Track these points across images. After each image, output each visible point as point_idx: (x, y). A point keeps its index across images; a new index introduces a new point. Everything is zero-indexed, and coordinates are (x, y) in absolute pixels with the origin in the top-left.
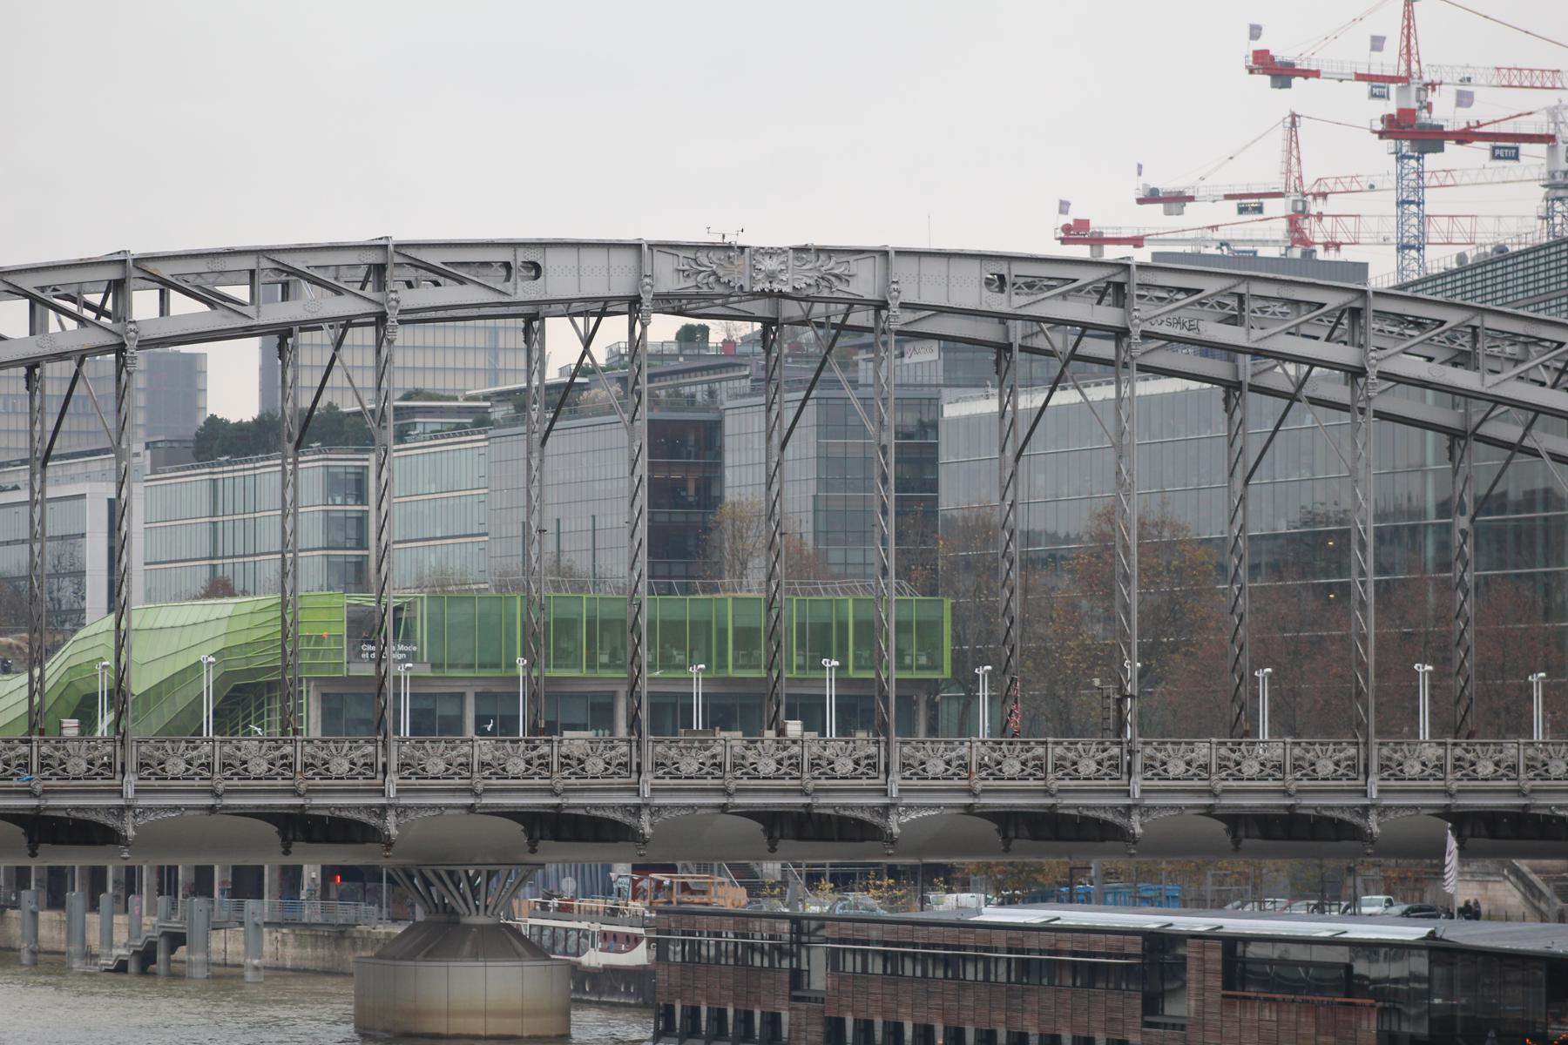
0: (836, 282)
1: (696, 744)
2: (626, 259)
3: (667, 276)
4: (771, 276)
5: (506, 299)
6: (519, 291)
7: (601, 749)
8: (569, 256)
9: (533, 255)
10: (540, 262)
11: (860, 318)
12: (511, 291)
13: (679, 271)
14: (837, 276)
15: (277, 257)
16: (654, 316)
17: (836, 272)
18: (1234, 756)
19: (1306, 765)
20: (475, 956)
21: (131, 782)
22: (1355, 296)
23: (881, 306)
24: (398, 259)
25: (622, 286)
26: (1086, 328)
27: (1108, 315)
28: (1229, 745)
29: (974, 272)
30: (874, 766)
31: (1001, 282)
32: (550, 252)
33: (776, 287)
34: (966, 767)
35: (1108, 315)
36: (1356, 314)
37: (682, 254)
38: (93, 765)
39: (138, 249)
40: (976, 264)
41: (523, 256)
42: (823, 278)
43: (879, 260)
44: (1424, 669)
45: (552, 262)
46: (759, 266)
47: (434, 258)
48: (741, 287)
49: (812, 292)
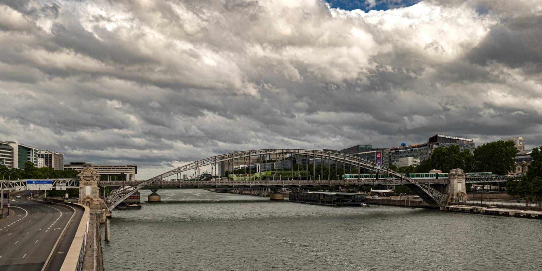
2: (282, 150)
3: (284, 151)
11: (297, 154)
21: (250, 183)
23: (298, 153)
25: (281, 152)
26: (312, 154)
27: (313, 153)
29: (304, 151)
31: (306, 151)
35: (313, 153)
44: (319, 176)
45: (277, 150)
47: (269, 150)
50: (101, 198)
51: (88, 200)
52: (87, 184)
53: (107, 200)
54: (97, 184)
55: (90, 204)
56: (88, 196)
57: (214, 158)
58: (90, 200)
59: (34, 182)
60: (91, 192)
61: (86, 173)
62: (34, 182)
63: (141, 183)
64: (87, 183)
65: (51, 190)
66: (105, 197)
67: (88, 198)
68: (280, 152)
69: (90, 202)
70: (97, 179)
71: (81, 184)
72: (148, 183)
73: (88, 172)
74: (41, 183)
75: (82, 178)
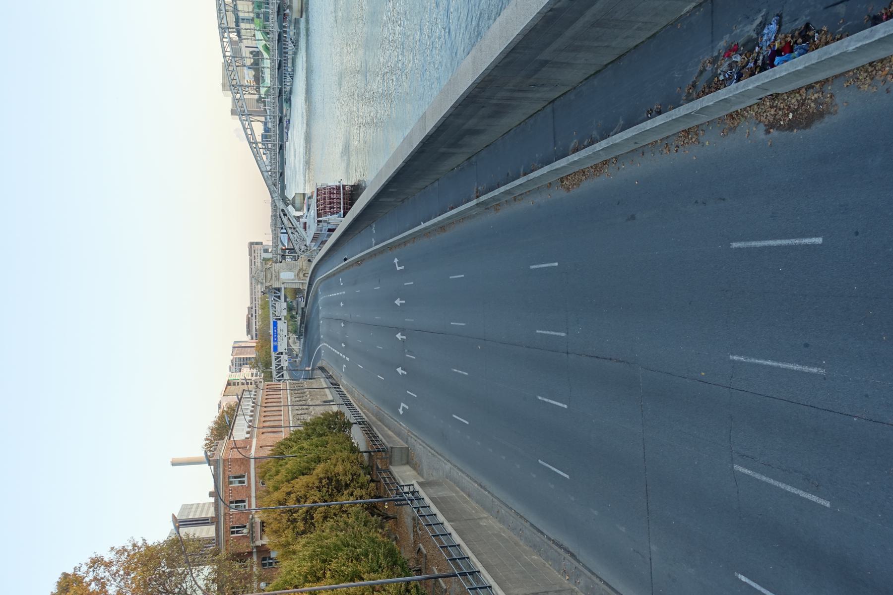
20: (292, 4)
39: (218, 26)
50: (298, 258)
51: (301, 275)
52: (278, 277)
53: (302, 251)
54: (277, 264)
55: (307, 272)
56: (295, 276)
57: (232, 88)
58: (300, 273)
59: (276, 343)
60: (290, 271)
61: (260, 279)
62: (276, 343)
63: (275, 203)
64: (276, 276)
65: (286, 321)
66: (296, 253)
67: (298, 275)
69: (304, 272)
70: (270, 264)
71: (276, 285)
72: (276, 192)
73: (259, 276)
74: (277, 334)
75: (268, 284)
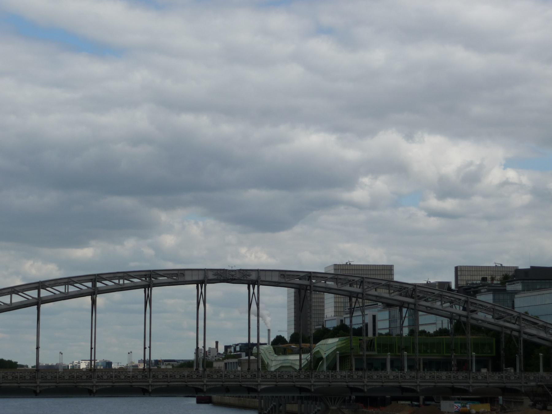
0: (247, 276)
1: (216, 372)
4: (233, 276)
5: (176, 281)
6: (179, 279)
7: (303, 373)
8: (190, 272)
9: (182, 272)
10: (184, 273)
12: (178, 279)
13: (213, 275)
14: (247, 275)
15: (156, 272)
16: (207, 284)
17: (247, 274)
18: (318, 374)
19: (334, 376)
22: (361, 278)
24: (153, 273)
25: (201, 278)
28: (334, 372)
30: (255, 376)
32: (186, 271)
33: (234, 277)
34: (381, 377)
36: (362, 282)
37: (214, 271)
38: (198, 376)
40: (278, 273)
41: (180, 272)
42: (244, 276)
43: (203, 271)
45: (186, 272)
46: (230, 273)
48: (227, 278)
49: (242, 278)
68: (195, 278)
